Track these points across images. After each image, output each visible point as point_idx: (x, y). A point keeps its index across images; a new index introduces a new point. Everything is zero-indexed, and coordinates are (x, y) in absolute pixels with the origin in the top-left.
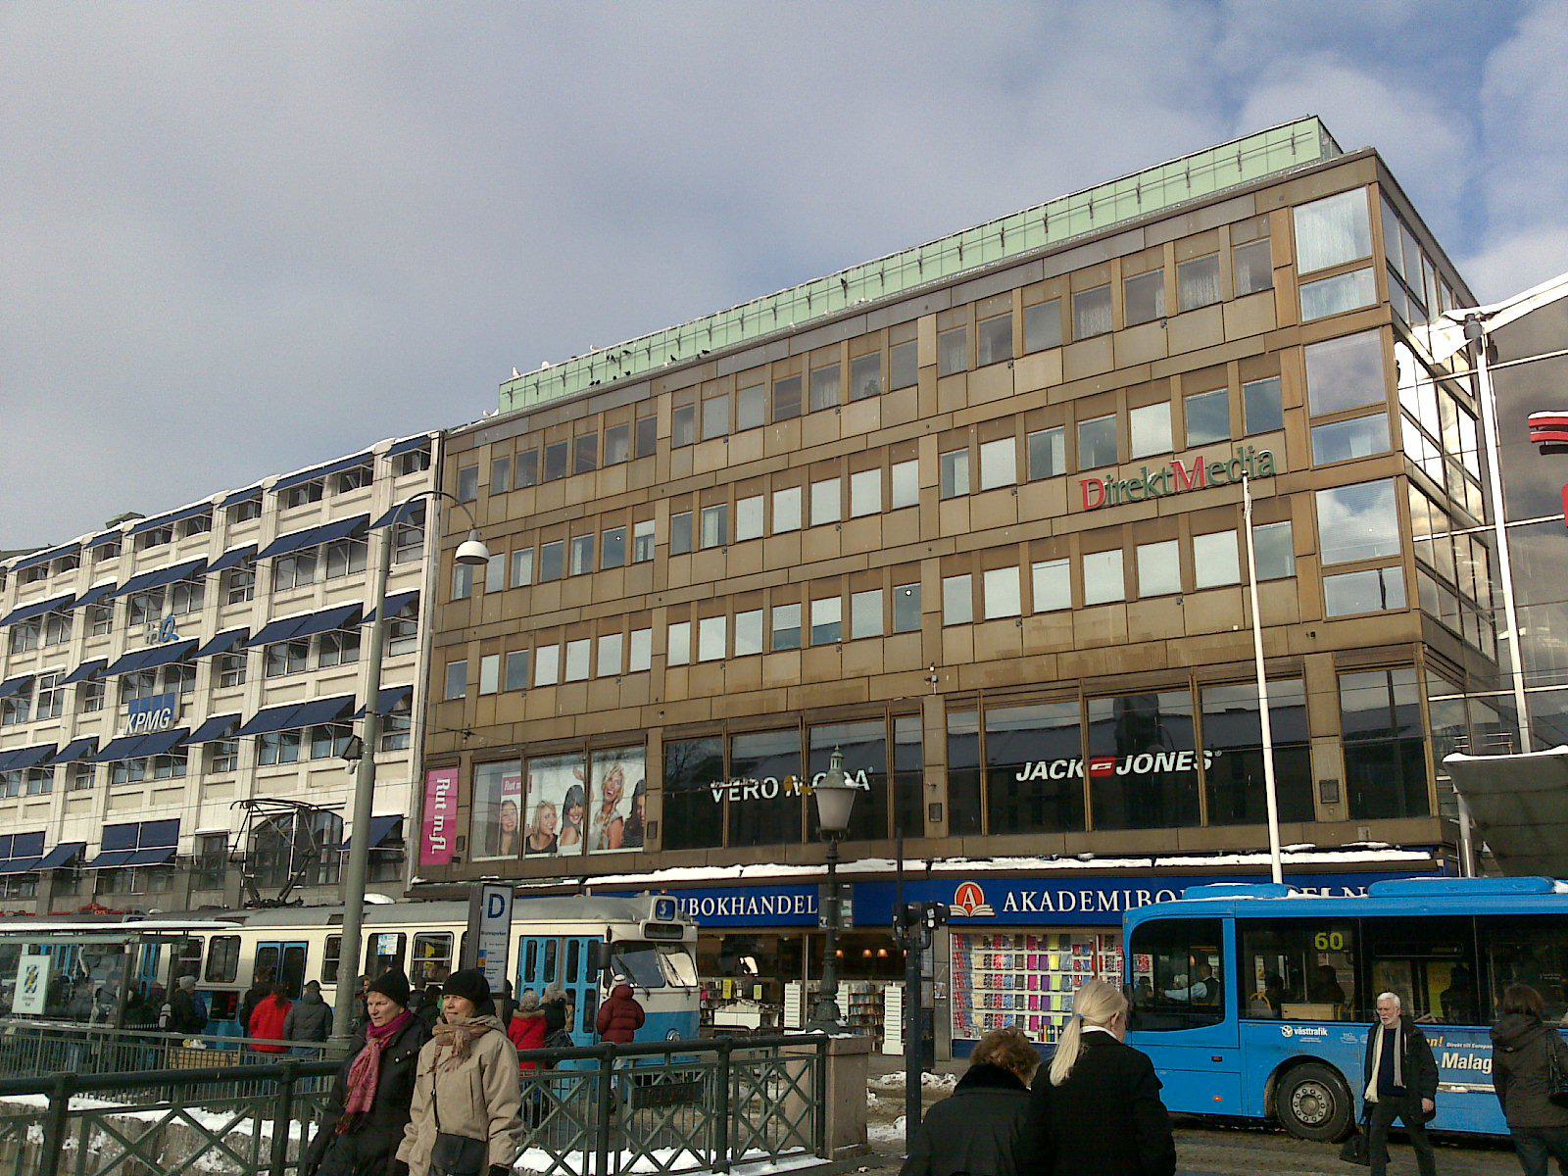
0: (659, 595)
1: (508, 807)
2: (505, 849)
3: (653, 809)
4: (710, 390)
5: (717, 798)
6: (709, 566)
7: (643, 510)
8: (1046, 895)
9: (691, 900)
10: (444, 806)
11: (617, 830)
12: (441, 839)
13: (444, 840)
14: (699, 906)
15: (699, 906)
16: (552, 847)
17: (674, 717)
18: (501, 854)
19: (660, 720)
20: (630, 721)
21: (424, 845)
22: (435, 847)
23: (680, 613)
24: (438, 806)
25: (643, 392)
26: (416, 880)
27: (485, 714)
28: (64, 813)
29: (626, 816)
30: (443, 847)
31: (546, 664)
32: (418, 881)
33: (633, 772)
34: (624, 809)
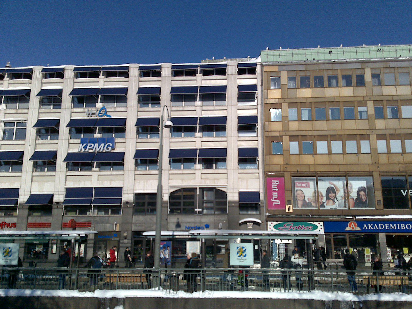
0: (372, 130)
1: (299, 192)
2: (300, 205)
3: (379, 195)
4: (387, 71)
5: (404, 194)
6: (393, 124)
7: (363, 103)
8: (376, 225)
9: (402, 225)
10: (277, 190)
11: (351, 202)
12: (277, 201)
13: (279, 201)
14: (405, 226)
15: (405, 226)
16: (323, 205)
17: (383, 169)
18: (298, 207)
19: (377, 169)
20: (367, 169)
21: (270, 203)
22: (274, 203)
23: (381, 137)
24: (273, 190)
25: (358, 66)
26: (267, 214)
27: (294, 160)
28: (32, 181)
29: (355, 198)
30: (279, 203)
31: (322, 147)
32: (269, 214)
33: (357, 185)
34: (354, 195)
